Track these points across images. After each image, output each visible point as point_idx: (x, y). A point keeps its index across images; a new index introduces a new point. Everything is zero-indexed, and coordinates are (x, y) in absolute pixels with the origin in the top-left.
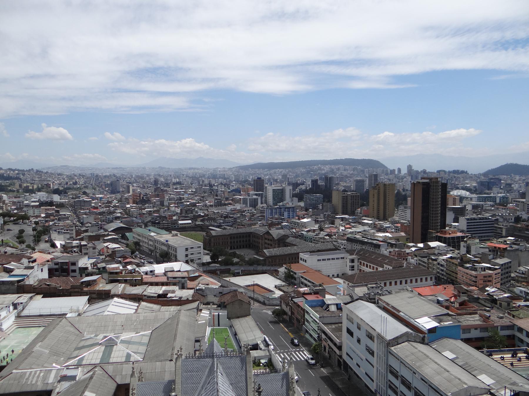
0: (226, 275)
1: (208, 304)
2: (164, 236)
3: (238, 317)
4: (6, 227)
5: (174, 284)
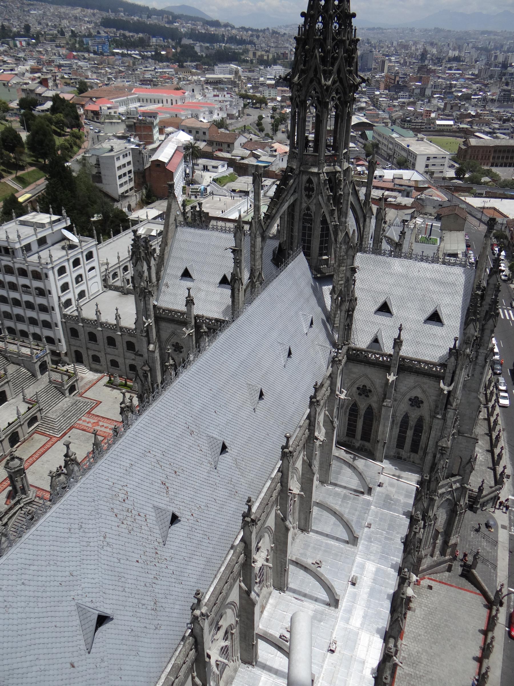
0: (465, 194)
1: (426, 214)
2: (407, 139)
3: (451, 231)
4: (247, 111)
5: (400, 191)
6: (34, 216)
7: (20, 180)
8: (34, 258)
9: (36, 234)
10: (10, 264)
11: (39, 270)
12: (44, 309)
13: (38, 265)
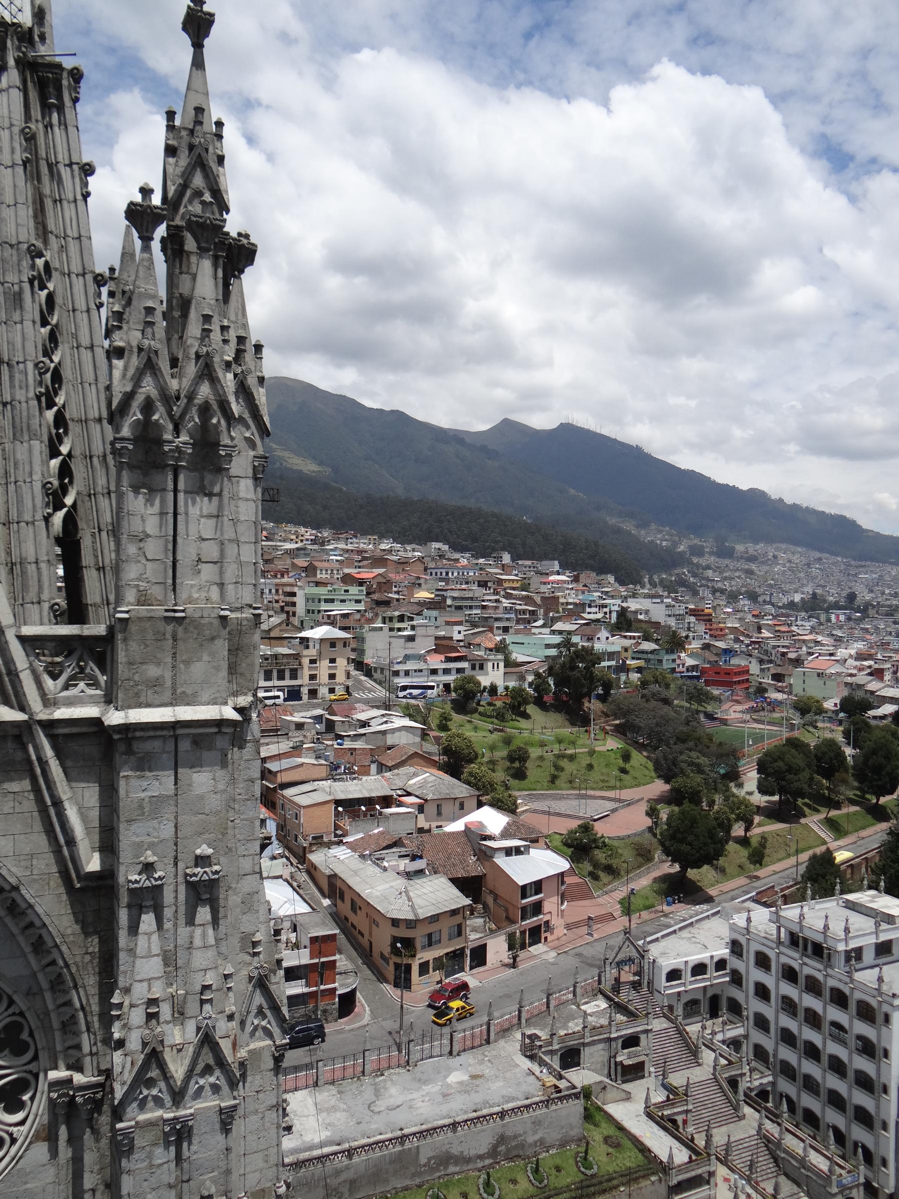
6: (873, 897)
7: (833, 825)
8: (867, 977)
9: (877, 933)
10: (820, 976)
11: (873, 1003)
12: (865, 1082)
13: (875, 993)
